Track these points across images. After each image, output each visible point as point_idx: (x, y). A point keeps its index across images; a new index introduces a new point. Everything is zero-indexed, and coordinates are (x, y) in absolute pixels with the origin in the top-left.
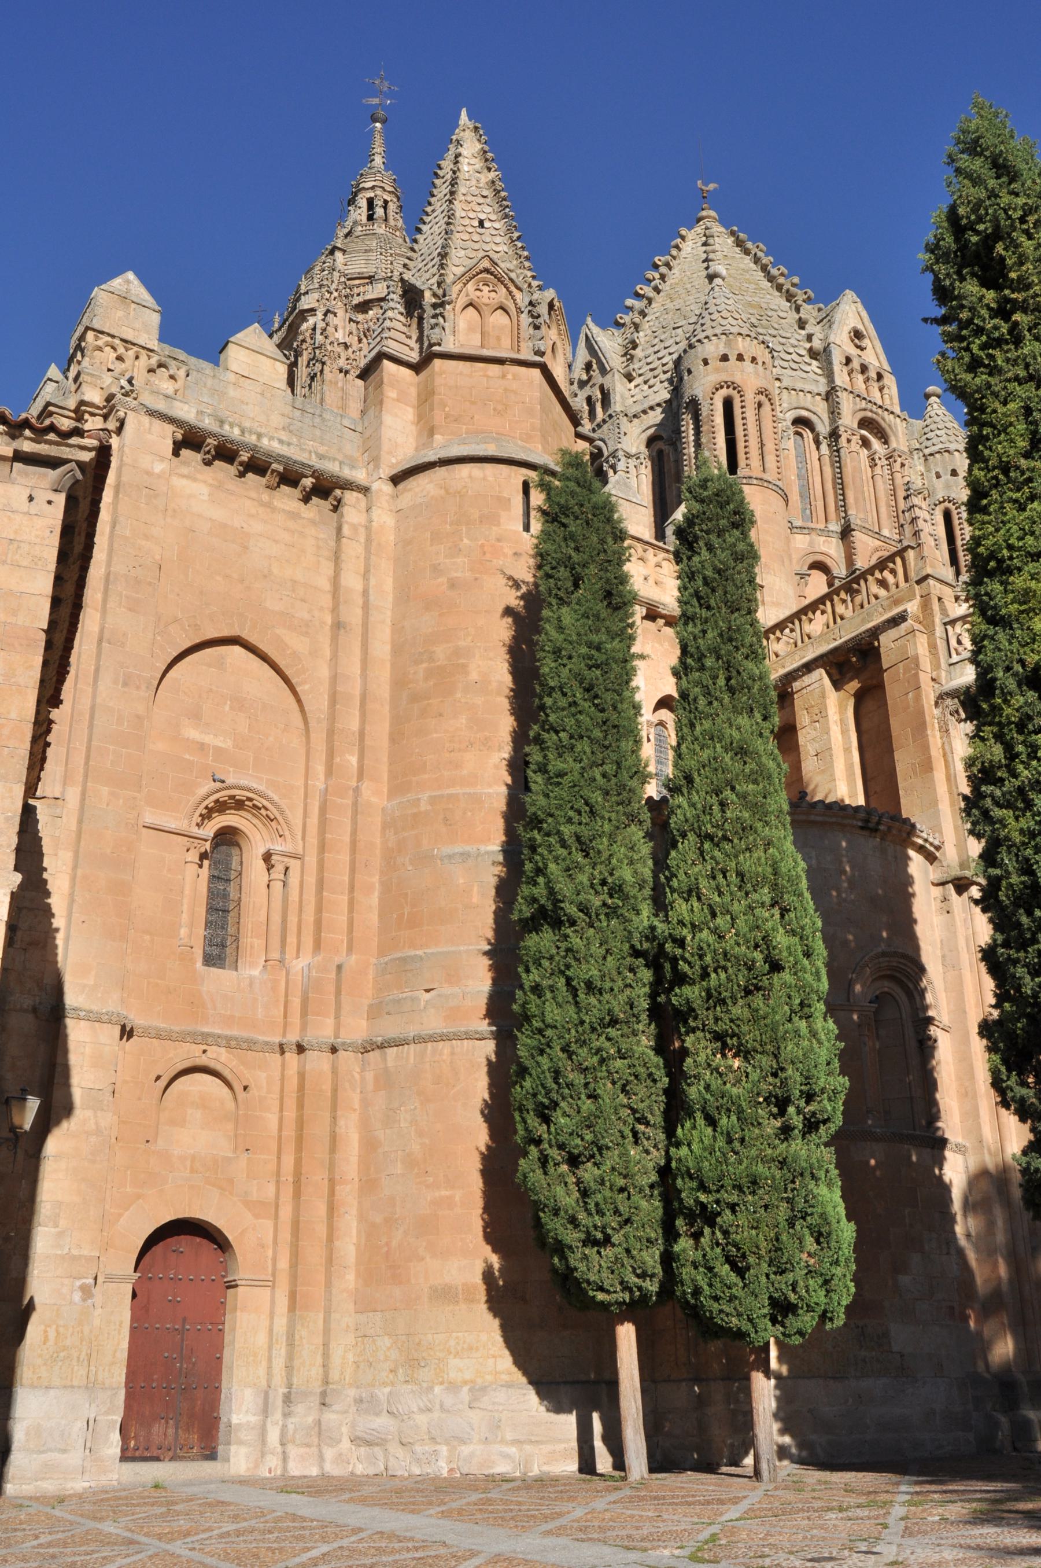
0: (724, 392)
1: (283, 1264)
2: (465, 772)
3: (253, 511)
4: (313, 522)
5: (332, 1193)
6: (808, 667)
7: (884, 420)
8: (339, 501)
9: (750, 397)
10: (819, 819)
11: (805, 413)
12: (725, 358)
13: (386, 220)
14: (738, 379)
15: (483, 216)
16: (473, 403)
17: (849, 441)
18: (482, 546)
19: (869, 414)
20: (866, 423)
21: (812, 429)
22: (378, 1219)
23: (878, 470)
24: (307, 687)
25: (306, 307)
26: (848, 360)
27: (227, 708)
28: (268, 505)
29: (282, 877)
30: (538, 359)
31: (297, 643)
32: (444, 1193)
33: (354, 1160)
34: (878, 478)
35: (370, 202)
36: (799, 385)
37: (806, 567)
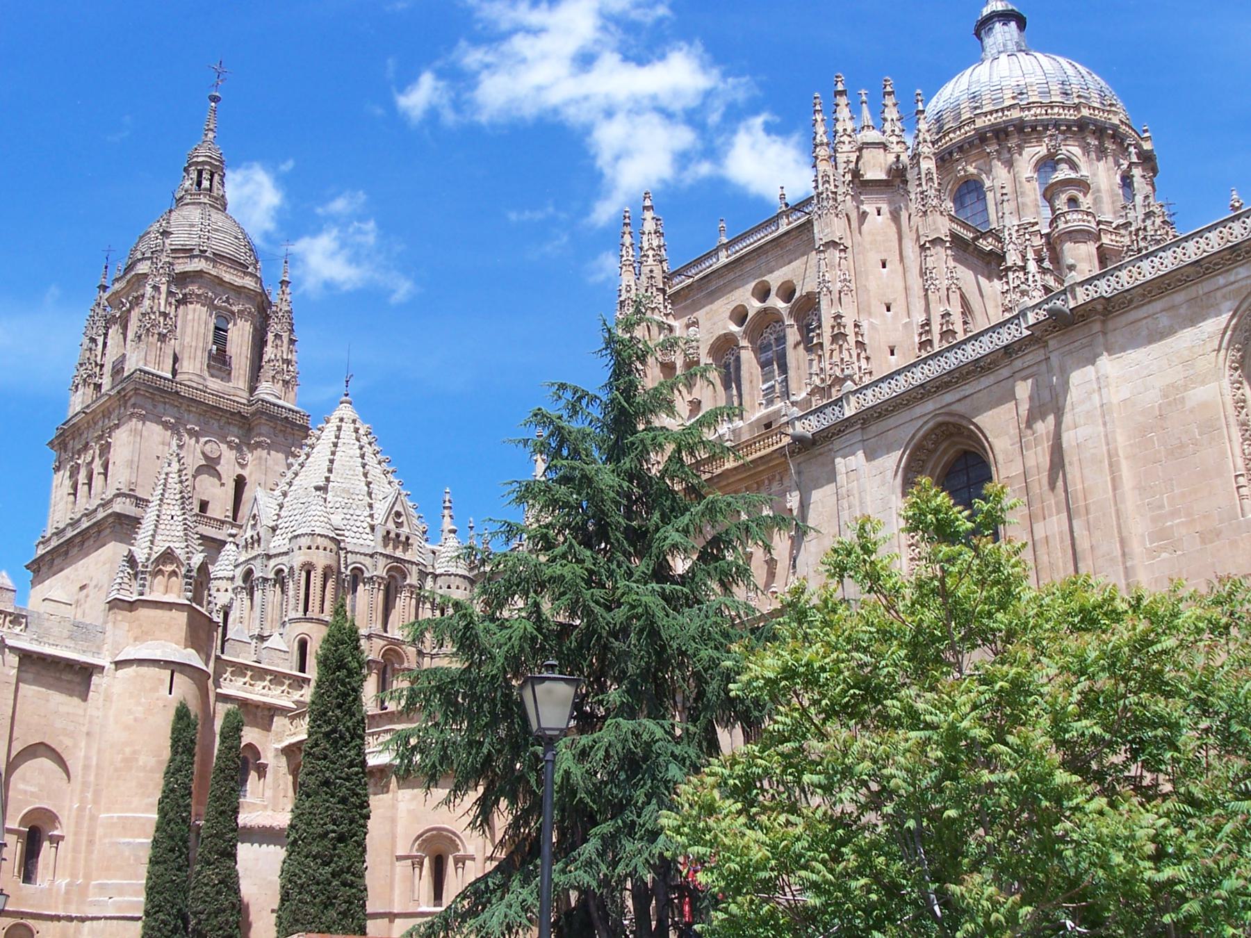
0: (306, 567)
4: (79, 684)
9: (320, 571)
12: (309, 548)
13: (210, 190)
14: (314, 562)
15: (173, 513)
25: (141, 272)
35: (200, 173)
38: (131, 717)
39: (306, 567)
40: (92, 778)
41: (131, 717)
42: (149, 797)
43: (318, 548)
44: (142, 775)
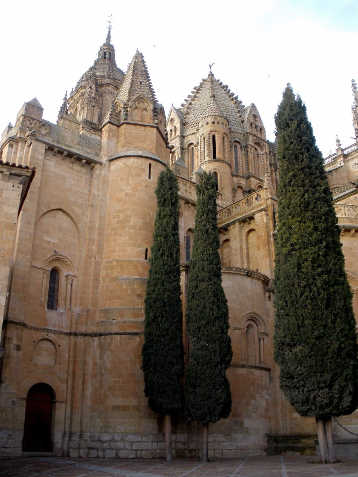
1: (69, 397)
2: (128, 253)
3: (67, 170)
4: (85, 173)
5: (84, 377)
6: (234, 223)
8: (93, 167)
10: (233, 272)
11: (238, 140)
12: (213, 123)
15: (141, 81)
16: (136, 138)
17: (251, 149)
18: (136, 183)
19: (257, 141)
20: (256, 143)
22: (97, 385)
23: (259, 158)
24: (81, 224)
27: (57, 231)
28: (72, 168)
29: (71, 283)
30: (156, 125)
31: (77, 210)
32: (117, 379)
33: (91, 368)
34: (259, 161)
36: (236, 131)
37: (236, 188)
38: (123, 193)
39: (212, 133)
40: (96, 236)
41: (123, 193)
42: (138, 246)
43: (218, 123)
44: (133, 231)
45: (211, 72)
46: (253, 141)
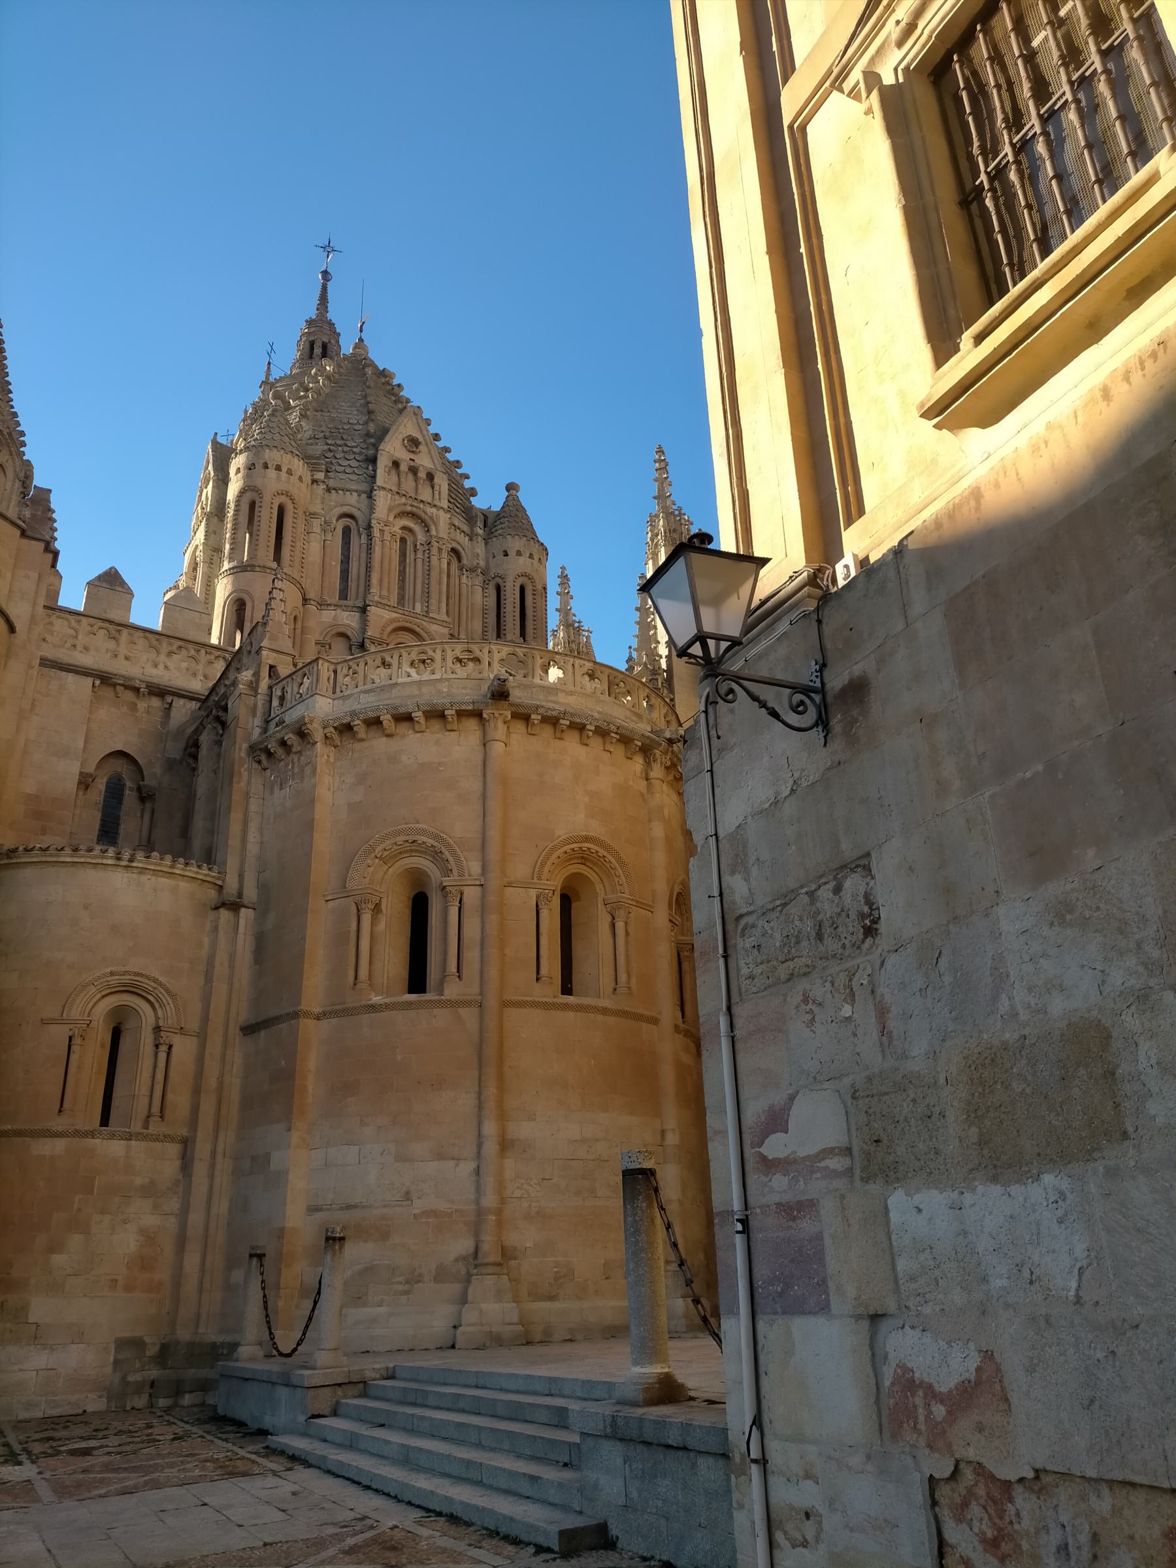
7: (425, 513)
17: (382, 531)
19: (409, 509)
21: (356, 522)
26: (396, 464)
34: (419, 562)
45: (361, 340)
46: (390, 509)
